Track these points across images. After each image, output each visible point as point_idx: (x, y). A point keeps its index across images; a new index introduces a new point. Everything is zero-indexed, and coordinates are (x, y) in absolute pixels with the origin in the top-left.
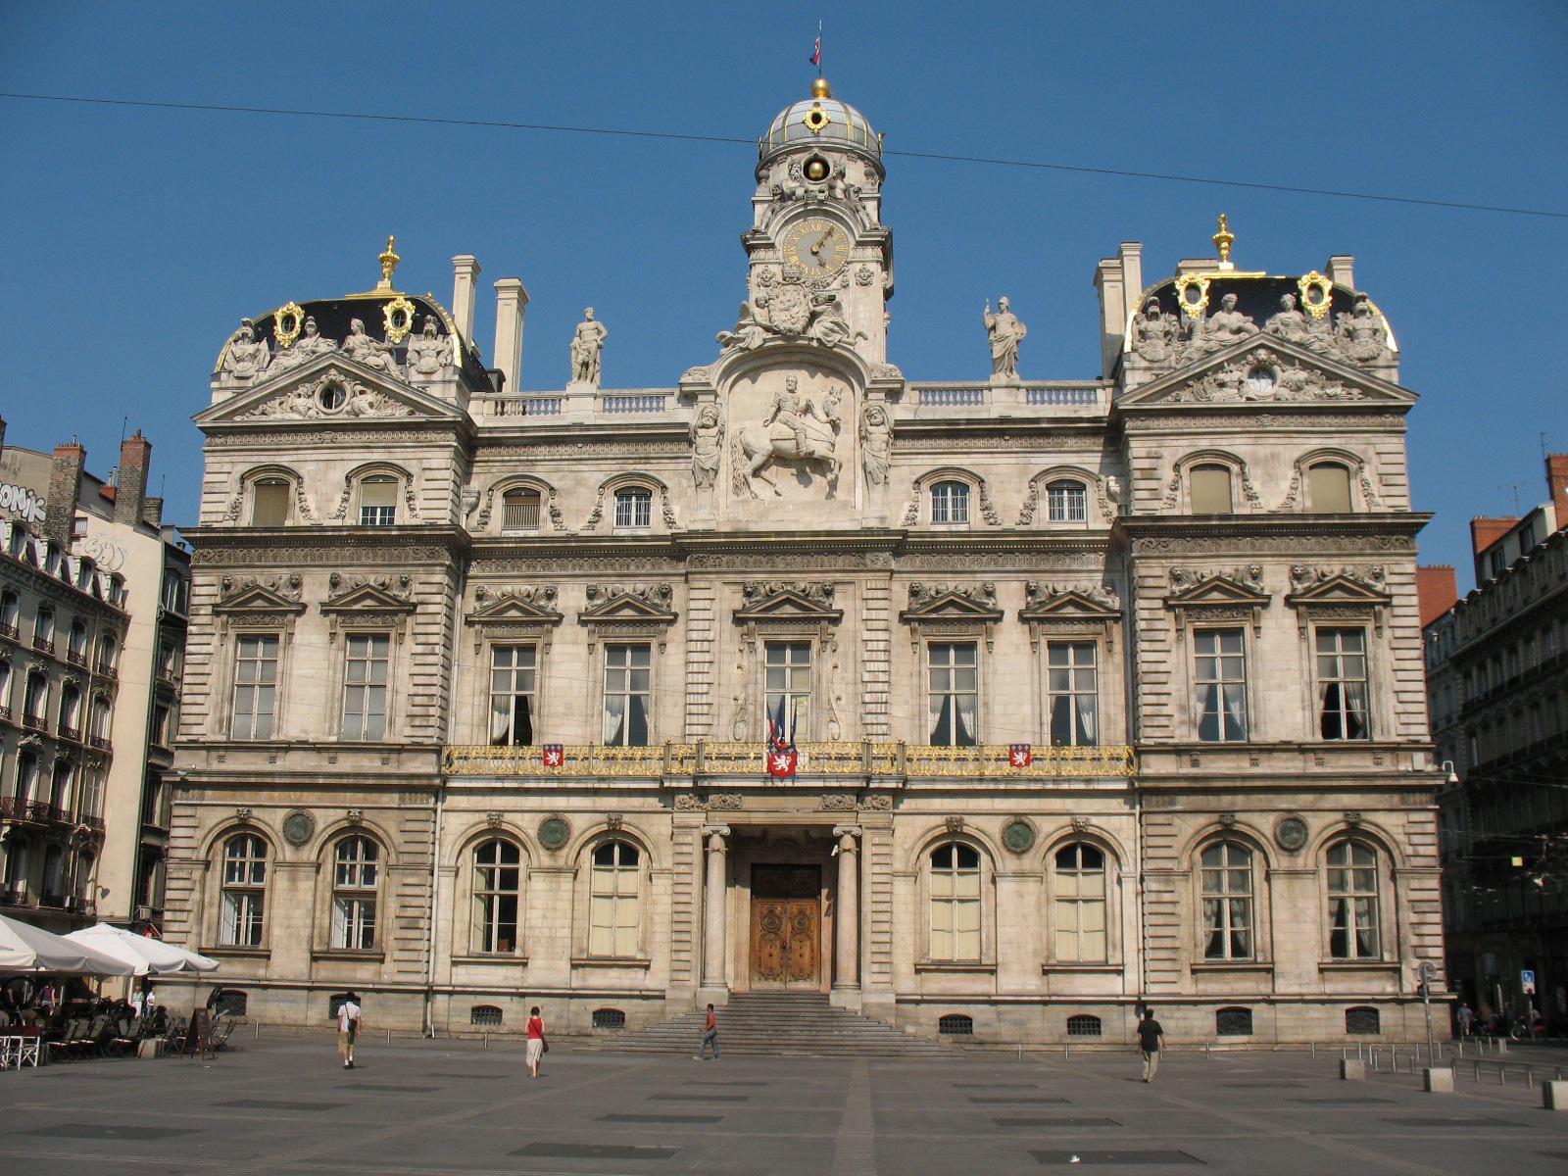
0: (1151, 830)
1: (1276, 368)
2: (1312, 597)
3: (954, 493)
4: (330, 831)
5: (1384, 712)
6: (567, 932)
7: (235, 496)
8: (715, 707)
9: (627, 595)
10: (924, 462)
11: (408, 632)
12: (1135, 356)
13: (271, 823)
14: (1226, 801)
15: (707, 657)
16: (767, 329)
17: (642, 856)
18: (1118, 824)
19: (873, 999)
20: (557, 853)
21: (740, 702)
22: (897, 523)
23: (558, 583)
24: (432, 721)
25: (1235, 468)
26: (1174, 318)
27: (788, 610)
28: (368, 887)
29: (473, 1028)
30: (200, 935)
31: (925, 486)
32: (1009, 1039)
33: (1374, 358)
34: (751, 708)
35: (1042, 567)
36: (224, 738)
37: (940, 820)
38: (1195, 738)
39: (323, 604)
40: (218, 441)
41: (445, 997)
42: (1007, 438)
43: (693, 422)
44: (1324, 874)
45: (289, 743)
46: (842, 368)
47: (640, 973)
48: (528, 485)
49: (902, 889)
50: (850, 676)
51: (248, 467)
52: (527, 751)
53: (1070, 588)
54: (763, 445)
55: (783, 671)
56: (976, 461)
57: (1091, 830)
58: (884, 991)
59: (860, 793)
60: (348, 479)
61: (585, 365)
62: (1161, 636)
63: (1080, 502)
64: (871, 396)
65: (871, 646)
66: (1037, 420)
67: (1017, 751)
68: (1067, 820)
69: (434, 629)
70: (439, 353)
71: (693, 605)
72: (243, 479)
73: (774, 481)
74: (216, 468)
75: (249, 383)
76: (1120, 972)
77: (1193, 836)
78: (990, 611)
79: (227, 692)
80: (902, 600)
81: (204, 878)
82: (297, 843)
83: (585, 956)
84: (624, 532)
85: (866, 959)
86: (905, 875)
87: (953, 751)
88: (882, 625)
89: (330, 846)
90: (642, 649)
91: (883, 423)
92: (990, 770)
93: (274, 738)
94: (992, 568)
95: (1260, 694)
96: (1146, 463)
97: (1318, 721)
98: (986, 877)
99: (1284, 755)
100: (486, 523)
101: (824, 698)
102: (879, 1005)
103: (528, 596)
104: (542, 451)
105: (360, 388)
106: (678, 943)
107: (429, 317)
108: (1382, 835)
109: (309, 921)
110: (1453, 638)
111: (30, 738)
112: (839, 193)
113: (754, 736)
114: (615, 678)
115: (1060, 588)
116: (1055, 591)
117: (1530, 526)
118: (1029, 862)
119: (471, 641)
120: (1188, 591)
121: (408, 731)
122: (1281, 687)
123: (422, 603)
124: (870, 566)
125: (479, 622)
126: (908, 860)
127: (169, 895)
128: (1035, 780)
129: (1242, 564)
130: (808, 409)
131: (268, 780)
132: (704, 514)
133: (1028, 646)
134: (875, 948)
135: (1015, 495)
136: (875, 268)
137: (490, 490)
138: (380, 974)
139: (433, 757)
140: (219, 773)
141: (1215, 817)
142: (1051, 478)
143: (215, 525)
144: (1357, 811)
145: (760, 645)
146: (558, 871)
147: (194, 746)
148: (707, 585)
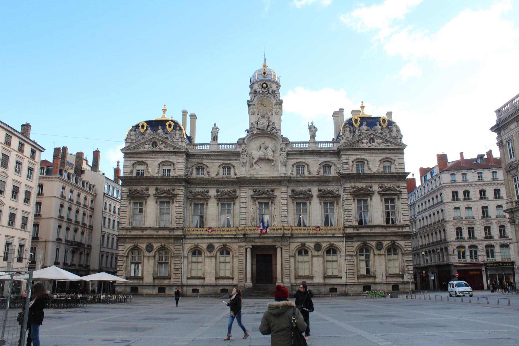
0: (348, 245)
1: (375, 139)
2: (384, 192)
3: (301, 167)
4: (157, 248)
5: (400, 218)
6: (214, 271)
7: (131, 169)
8: (247, 218)
9: (226, 192)
10: (295, 160)
11: (175, 201)
12: (343, 136)
13: (143, 247)
14: (364, 239)
15: (245, 206)
16: (258, 129)
17: (231, 253)
18: (341, 245)
19: (285, 285)
20: (212, 253)
21: (253, 216)
22: (289, 174)
23: (209, 189)
24: (181, 222)
25: (366, 162)
26: (352, 127)
27: (264, 196)
28: (166, 261)
29: (192, 294)
30: (126, 274)
31: (295, 166)
32: (316, 293)
33: (397, 137)
34: (255, 218)
35: (322, 185)
36: (131, 227)
37: (300, 244)
38: (357, 224)
39: (154, 195)
40: (127, 155)
41: (186, 287)
44: (387, 255)
45: (147, 228)
46: (275, 138)
47: (231, 280)
48: (201, 166)
49: (292, 260)
50: (278, 210)
51: (134, 162)
52: (204, 229)
53: (328, 190)
55: (263, 209)
57: (334, 245)
58: (288, 283)
59: (282, 237)
60: (159, 165)
61: (215, 137)
62: (350, 201)
63: (330, 169)
64: (282, 145)
65: (283, 203)
66: (320, 151)
67: (317, 228)
68: (329, 243)
69: (181, 200)
70: (180, 134)
71: (241, 194)
72: (133, 165)
73: (259, 165)
74: (127, 162)
75: (134, 141)
76: (341, 278)
77: (357, 247)
78: (310, 195)
79: (131, 216)
80: (290, 193)
81: (126, 260)
83: (218, 276)
84: (225, 176)
85: (284, 276)
86: (292, 256)
87: (302, 228)
88: (286, 198)
89: (157, 252)
90: (229, 205)
92: (311, 232)
93: (143, 227)
95: (372, 214)
96: (346, 161)
97: (385, 220)
98: (310, 256)
99: (377, 228)
100: (192, 175)
101: (272, 215)
102: (287, 286)
103: (202, 192)
104: (205, 157)
105: (161, 143)
106: (240, 273)
107: (178, 126)
108: (400, 246)
109: (152, 270)
110: (415, 196)
111: (76, 226)
112: (270, 92)
113: (256, 224)
115: (326, 190)
116: (325, 190)
117: (433, 170)
118: (320, 253)
119: (189, 203)
120: (355, 191)
121: (175, 225)
122: (377, 212)
123: (178, 194)
124: (283, 185)
125: (191, 198)
126: (293, 253)
127: (118, 264)
128: (321, 234)
129: (368, 184)
130: (266, 148)
131: (142, 237)
132: (244, 172)
133: (319, 204)
134: (286, 273)
136: (278, 110)
137: (193, 167)
138: (170, 282)
139: (182, 231)
140: (130, 235)
141: (362, 242)
142: (324, 164)
143: (127, 176)
144: (394, 241)
145: (257, 203)
146: (212, 257)
147: (123, 229)
148: (245, 189)
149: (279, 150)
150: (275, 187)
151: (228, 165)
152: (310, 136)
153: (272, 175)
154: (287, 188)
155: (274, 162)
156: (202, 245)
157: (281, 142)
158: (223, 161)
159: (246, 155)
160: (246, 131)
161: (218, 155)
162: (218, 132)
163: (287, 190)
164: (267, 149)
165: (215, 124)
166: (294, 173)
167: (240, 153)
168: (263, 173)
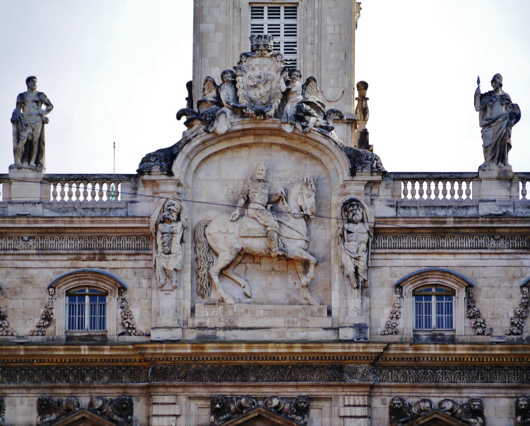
3: (439, 297)
10: (407, 263)
23: (5, 395)
31: (408, 289)
42: (497, 237)
56: (464, 263)
61: (29, 144)
73: (241, 281)
91: (362, 221)
94: (478, 384)
132: (165, 321)
135: (506, 301)
148: (172, 399)
149: (336, 212)
150: (314, 391)
151: (92, 283)
152: (485, 148)
153: (300, 335)
154: (370, 396)
155: (312, 269)
157: (346, 175)
158: (68, 264)
159: (177, 239)
160: (179, 117)
161: (44, 232)
162: (45, 121)
163: (369, 406)
164: (281, 206)
165: (31, 81)
166: (400, 327)
167: (152, 226)
168: (258, 323)
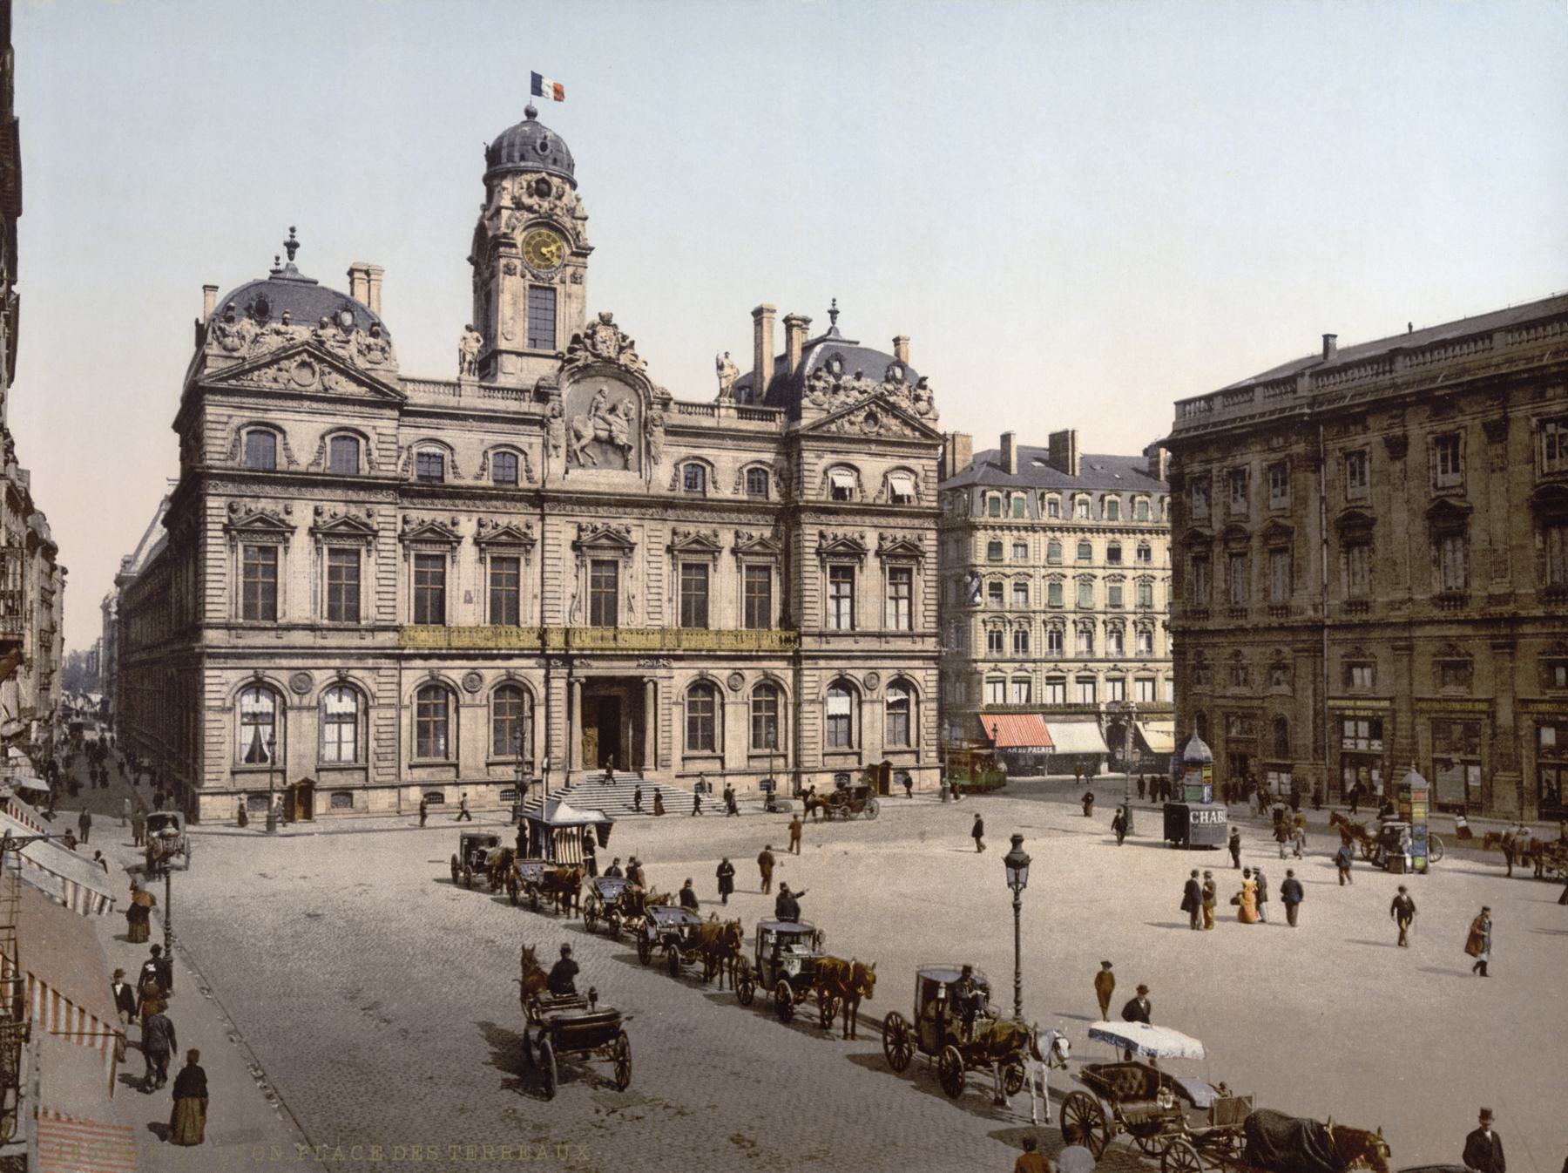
4: (325, 684)
43: (548, 413)
54: (588, 433)
60: (322, 437)
82: (300, 692)
105: (327, 370)
114: (495, 580)
133: (735, 569)
156: (449, 673)
